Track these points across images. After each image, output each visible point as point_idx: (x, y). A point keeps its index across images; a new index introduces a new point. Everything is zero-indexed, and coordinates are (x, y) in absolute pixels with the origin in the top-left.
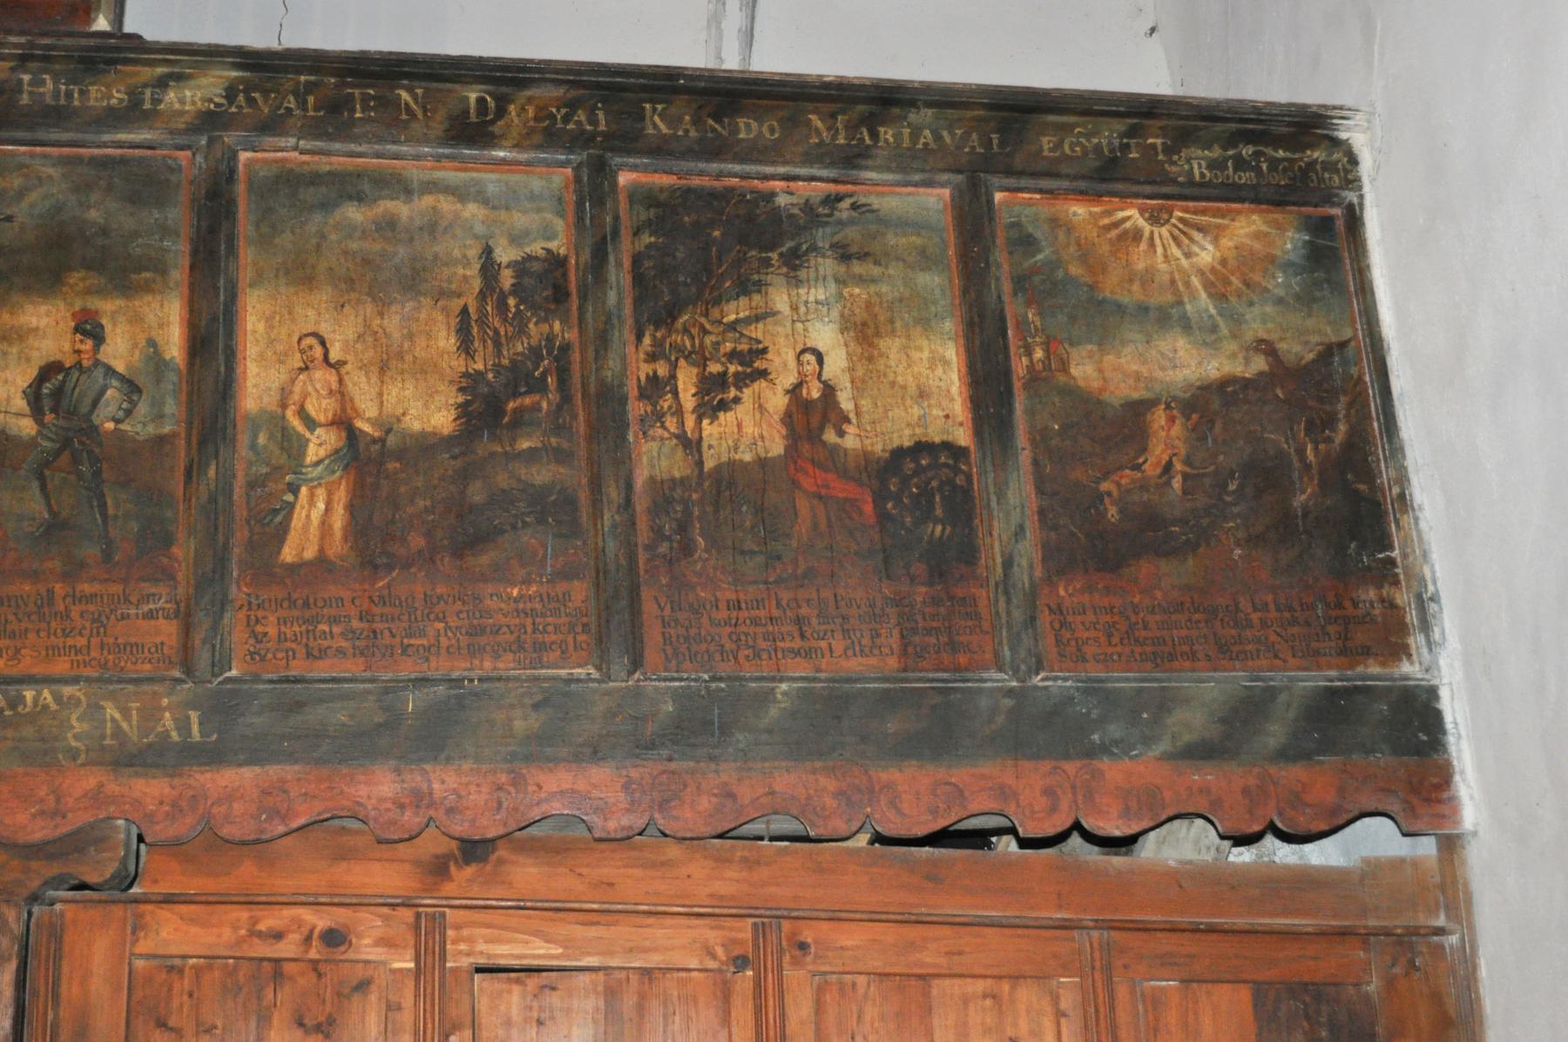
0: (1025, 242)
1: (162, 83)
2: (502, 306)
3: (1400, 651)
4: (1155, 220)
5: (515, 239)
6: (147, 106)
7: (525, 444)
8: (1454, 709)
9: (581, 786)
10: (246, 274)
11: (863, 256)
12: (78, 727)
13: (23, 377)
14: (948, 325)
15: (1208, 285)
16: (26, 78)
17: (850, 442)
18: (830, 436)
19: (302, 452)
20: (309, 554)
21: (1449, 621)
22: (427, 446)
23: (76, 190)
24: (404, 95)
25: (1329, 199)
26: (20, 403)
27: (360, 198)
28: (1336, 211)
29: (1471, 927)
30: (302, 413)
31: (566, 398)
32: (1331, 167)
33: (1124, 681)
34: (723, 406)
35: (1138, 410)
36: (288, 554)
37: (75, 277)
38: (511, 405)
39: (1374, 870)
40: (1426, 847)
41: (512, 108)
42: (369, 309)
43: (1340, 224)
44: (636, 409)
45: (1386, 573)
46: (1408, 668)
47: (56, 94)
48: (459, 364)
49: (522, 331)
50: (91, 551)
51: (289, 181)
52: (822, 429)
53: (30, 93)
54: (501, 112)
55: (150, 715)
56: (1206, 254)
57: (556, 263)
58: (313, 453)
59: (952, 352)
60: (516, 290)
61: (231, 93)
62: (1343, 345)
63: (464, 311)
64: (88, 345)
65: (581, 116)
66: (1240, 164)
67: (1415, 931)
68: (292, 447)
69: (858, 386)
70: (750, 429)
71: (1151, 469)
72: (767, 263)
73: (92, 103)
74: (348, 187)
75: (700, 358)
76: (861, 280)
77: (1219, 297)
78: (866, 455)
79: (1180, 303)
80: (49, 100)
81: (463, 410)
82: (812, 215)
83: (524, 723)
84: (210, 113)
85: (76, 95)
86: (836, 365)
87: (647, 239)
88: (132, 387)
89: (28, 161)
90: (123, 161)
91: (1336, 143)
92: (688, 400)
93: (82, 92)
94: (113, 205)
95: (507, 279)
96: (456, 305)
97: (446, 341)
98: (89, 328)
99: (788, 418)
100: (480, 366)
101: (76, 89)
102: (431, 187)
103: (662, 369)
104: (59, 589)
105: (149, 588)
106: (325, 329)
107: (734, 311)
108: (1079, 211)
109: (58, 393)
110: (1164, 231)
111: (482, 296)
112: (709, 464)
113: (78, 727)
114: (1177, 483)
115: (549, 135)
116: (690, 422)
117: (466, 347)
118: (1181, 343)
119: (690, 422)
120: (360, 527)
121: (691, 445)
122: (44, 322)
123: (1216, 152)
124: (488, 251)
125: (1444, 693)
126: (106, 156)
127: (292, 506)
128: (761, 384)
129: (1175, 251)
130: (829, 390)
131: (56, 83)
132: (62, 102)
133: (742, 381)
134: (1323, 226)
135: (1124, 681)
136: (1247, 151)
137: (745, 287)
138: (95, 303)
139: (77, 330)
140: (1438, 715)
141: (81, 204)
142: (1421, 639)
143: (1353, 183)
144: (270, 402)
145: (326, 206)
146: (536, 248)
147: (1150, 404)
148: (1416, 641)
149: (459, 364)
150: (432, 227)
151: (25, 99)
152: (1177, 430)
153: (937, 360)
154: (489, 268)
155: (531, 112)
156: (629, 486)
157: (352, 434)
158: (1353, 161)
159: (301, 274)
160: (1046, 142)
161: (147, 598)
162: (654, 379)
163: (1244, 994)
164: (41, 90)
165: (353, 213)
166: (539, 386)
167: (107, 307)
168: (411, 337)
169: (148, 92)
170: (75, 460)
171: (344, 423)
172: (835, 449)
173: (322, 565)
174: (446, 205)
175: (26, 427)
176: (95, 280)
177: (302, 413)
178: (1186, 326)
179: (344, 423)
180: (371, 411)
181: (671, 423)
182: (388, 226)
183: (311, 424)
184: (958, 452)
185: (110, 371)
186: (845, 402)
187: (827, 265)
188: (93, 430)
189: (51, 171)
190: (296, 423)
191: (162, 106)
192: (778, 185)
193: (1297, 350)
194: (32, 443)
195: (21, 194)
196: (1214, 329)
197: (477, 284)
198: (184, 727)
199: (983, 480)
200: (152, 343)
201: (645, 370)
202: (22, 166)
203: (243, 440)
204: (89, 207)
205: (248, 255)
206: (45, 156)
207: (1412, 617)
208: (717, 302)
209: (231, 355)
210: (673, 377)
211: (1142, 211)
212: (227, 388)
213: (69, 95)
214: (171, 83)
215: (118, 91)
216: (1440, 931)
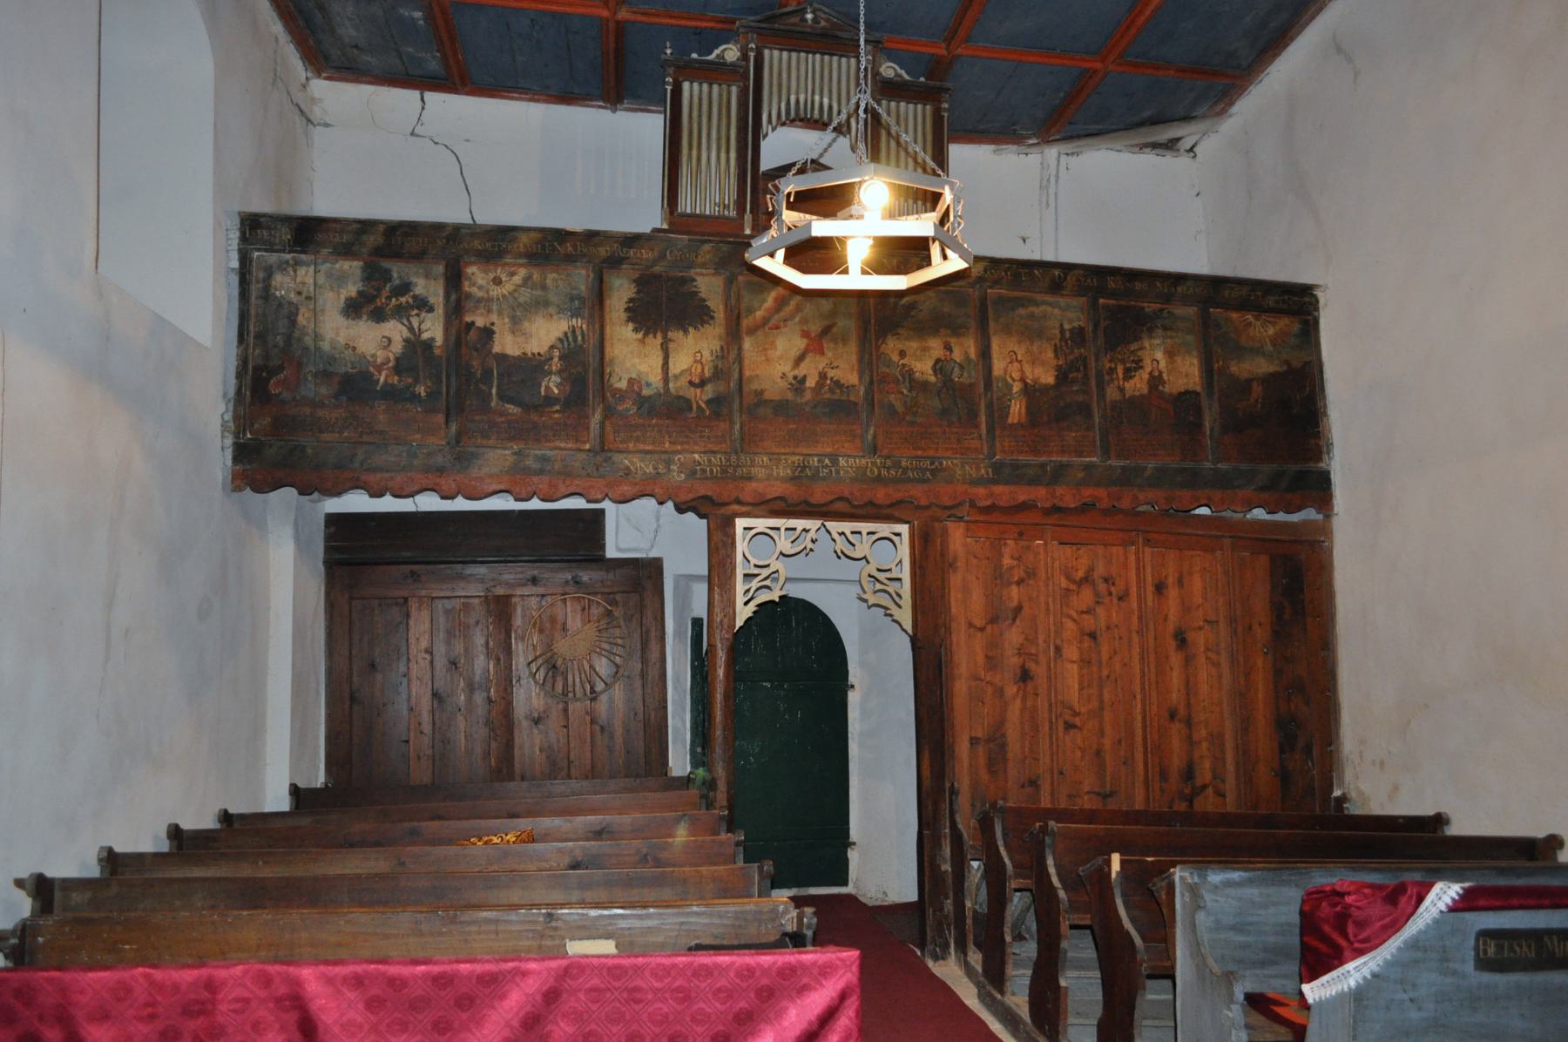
2: (1067, 343)
3: (1319, 459)
4: (1257, 318)
5: (1070, 321)
7: (1075, 388)
8: (1337, 479)
9: (1096, 493)
10: (991, 333)
11: (1171, 329)
12: (959, 472)
13: (930, 364)
14: (1195, 353)
15: (1271, 341)
17: (1167, 389)
18: (1161, 388)
19: (1011, 390)
20: (1016, 421)
21: (1337, 451)
22: (1046, 389)
24: (1036, 272)
25: (1310, 314)
26: (930, 372)
27: (1023, 306)
28: (1310, 318)
29: (1332, 542)
30: (1011, 377)
31: (1086, 376)
32: (1310, 303)
33: (1243, 466)
34: (1131, 377)
35: (1249, 381)
36: (1010, 421)
37: (942, 330)
38: (1071, 376)
39: (1305, 523)
40: (1320, 517)
41: (1069, 278)
42: (1028, 343)
43: (1311, 322)
44: (1107, 378)
45: (1317, 435)
48: (1055, 362)
49: (1073, 352)
50: (954, 418)
51: (1001, 300)
52: (1158, 386)
54: (1065, 279)
55: (978, 469)
56: (1271, 331)
57: (1081, 329)
58: (1015, 389)
59: (1195, 361)
60: (1070, 338)
61: (985, 271)
62: (1310, 362)
63: (1056, 345)
64: (948, 353)
65: (1089, 281)
66: (1284, 301)
67: (1316, 541)
68: (1010, 387)
69: (1169, 373)
70: (1138, 385)
71: (1252, 400)
72: (1142, 331)
74: (1021, 303)
75: (1123, 362)
76: (1171, 337)
77: (1274, 345)
78: (1170, 395)
79: (1262, 346)
81: (1057, 377)
83: (1081, 475)
84: (980, 278)
86: (1163, 364)
87: (1108, 322)
88: (961, 367)
90: (952, 292)
92: (1121, 376)
95: (1068, 335)
96: (1053, 343)
97: (1050, 354)
98: (948, 347)
99: (1149, 381)
100: (1061, 363)
102: (1044, 303)
103: (1113, 366)
104: (947, 430)
105: (972, 430)
106: (1016, 350)
108: (1234, 315)
109: (941, 369)
110: (1259, 323)
111: (1061, 340)
112: (1127, 396)
113: (959, 472)
114: (1259, 406)
115: (1081, 291)
116: (1121, 383)
117: (1056, 356)
118: (1263, 361)
119: (1121, 383)
120: (1030, 411)
121: (1122, 390)
122: (935, 345)
123: (1277, 298)
124: (1062, 325)
125: (1332, 473)
127: (1009, 406)
128: (1141, 371)
129: (1262, 330)
133: (1136, 369)
134: (1306, 322)
135: (1243, 466)
136: (1286, 297)
137: (1137, 338)
138: (948, 339)
139: (945, 348)
140: (1330, 480)
142: (1326, 456)
143: (1317, 309)
144: (1002, 373)
145: (1013, 309)
146: (1076, 324)
147: (1253, 380)
148: (1325, 457)
149: (1055, 362)
150: (1045, 316)
152: (1260, 388)
153: (1192, 364)
154: (1062, 331)
155: (1074, 279)
156: (1105, 401)
157: (1026, 384)
158: (1318, 302)
159: (1007, 331)
160: (1227, 293)
161: (971, 433)
162: (1111, 368)
165: (1022, 311)
166: (1078, 370)
167: (953, 340)
168: (1041, 353)
170: (948, 390)
171: (1023, 380)
172: (1162, 392)
173: (1020, 424)
174: (1049, 309)
175: (933, 379)
176: (949, 332)
177: (1011, 377)
178: (1264, 355)
179: (1023, 380)
180: (1031, 377)
181: (1116, 382)
182: (1032, 316)
183: (1014, 380)
184: (1197, 394)
185: (955, 362)
186: (1165, 376)
187: (1160, 332)
188: (952, 380)
190: (1010, 380)
192: (1146, 304)
193: (1296, 364)
194: (935, 384)
195: (924, 302)
196: (1272, 356)
197: (1059, 336)
198: (988, 474)
199: (1205, 402)
200: (966, 352)
201: (1108, 365)
203: (995, 385)
205: (992, 324)
207: (1325, 449)
208: (1129, 343)
209: (990, 358)
210: (1116, 368)
211: (1253, 316)
212: (988, 369)
216: (1323, 542)
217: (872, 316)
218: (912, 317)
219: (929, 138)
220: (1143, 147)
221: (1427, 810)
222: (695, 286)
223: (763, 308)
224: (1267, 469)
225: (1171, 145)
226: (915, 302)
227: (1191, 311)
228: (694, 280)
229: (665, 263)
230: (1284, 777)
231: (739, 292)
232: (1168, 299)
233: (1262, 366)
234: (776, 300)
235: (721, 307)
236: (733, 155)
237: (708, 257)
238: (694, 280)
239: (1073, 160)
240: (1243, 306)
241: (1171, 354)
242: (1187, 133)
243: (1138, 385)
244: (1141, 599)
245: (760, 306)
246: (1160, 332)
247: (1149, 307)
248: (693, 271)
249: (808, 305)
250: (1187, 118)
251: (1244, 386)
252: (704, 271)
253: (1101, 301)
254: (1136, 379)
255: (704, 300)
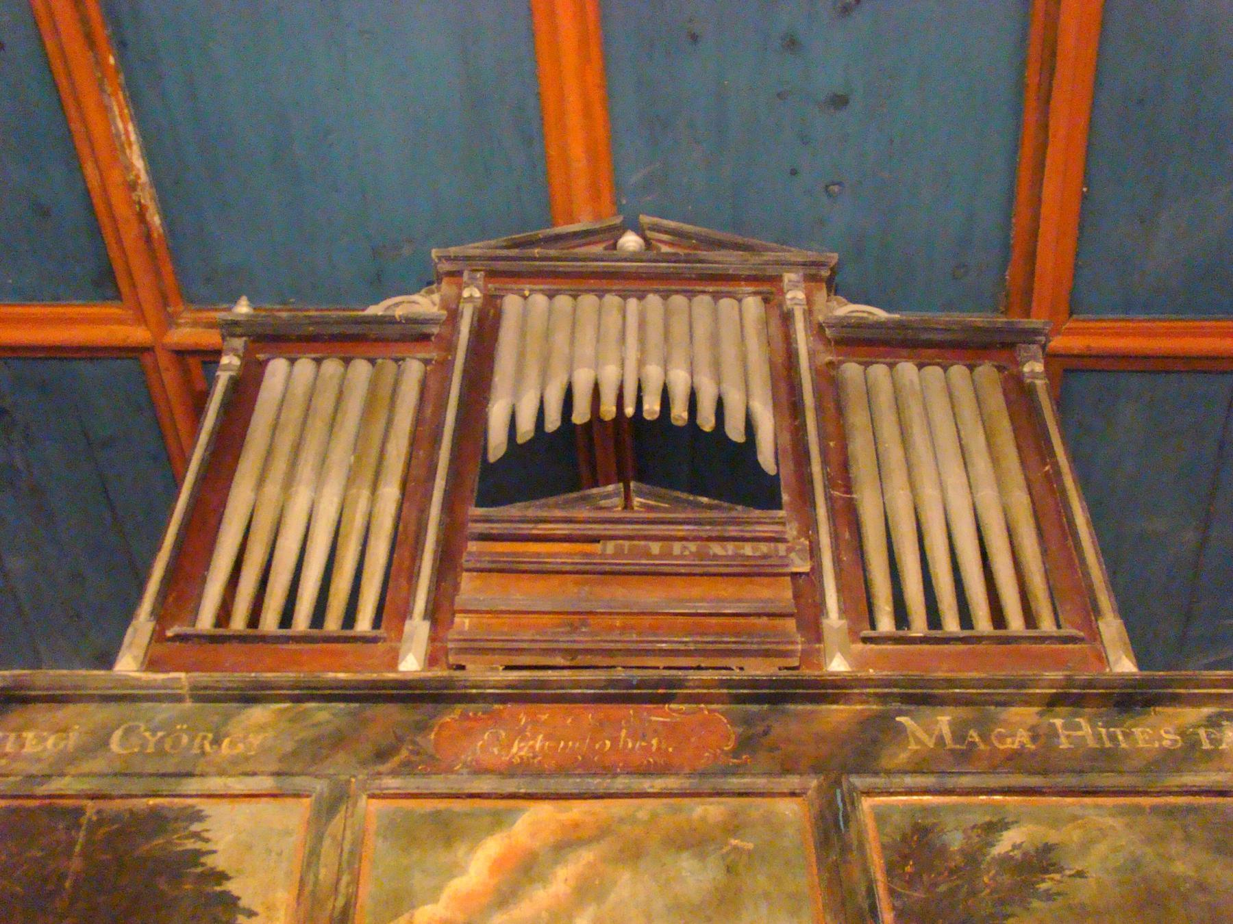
1: (1213, 722)
6: (1206, 746)
16: (1058, 722)
23: (1149, 841)
47: (1098, 738)
53: (1068, 737)
73: (1141, 744)
80: (1091, 743)
85: (1120, 737)
89: (1079, 812)
90: (1190, 809)
93: (1126, 735)
94: (1203, 857)
101: (1118, 731)
126: (1166, 805)
131: (1093, 727)
132: (1108, 745)
141: (1160, 856)
151: (1064, 744)
164: (1079, 733)
169: (1202, 732)
189: (1110, 821)
191: (1224, 746)
195: (1086, 846)
202: (1075, 818)
204: (1171, 859)
206: (1097, 806)
213: (1112, 737)
214: (1225, 723)
215: (1166, 732)
217: (881, 891)
218: (1049, 896)
219: (1004, 425)
222: (196, 835)
223: (445, 896)
226: (1048, 848)
228: (198, 816)
229: (98, 764)
231: (359, 843)
234: (498, 865)
235: (284, 896)
236: (390, 492)
237: (256, 740)
238: (198, 816)
245: (439, 888)
248: (193, 785)
249: (625, 876)
252: (238, 785)
255: (222, 877)
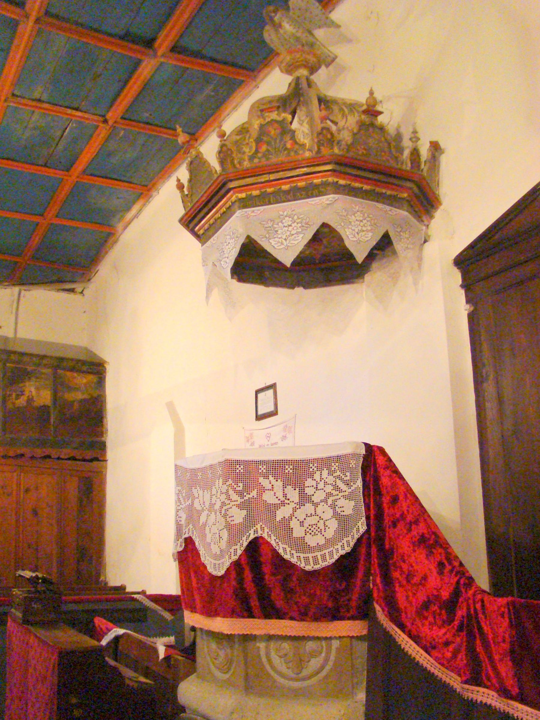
0: (61, 377)
45: (102, 426)
46: (103, 439)
56: (85, 381)
59: (49, 392)
66: (91, 369)
82: (32, 372)
86: (34, 393)
91: (104, 366)
107: (21, 385)
108: (68, 374)
110: (79, 377)
121: (14, 404)
130: (33, 397)
136: (92, 367)
140: (105, 446)
143: (105, 372)
148: (105, 435)
158: (106, 369)
162: (10, 394)
163: (77, 478)
184: (49, 407)
186: (35, 398)
187: (33, 379)
193: (95, 395)
199: (52, 411)
201: (8, 393)
207: (104, 432)
220: (58, 290)
221: (118, 584)
224: (78, 440)
225: (72, 291)
227: (49, 371)
230: (78, 571)
232: (39, 365)
233: (80, 396)
239: (27, 294)
240: (72, 370)
241: (37, 389)
242: (78, 287)
243: (22, 402)
244: (18, 494)
246: (33, 379)
247: (29, 368)
250: (73, 282)
251: (71, 404)
253: (8, 365)
254: (21, 400)
